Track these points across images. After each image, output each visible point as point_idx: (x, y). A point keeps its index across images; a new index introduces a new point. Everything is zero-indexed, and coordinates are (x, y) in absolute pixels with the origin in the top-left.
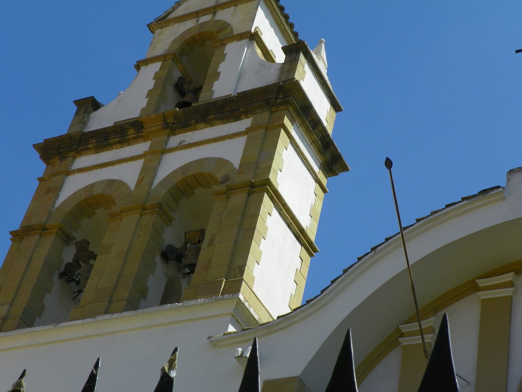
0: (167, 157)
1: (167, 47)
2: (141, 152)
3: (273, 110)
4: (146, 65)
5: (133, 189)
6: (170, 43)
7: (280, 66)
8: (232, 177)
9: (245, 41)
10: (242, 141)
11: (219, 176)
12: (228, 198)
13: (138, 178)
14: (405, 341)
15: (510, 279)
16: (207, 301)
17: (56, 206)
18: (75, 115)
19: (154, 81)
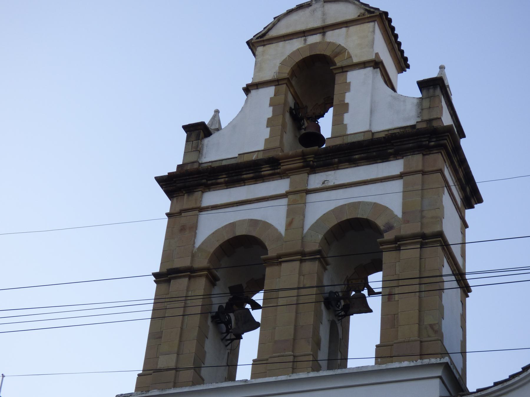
0: (311, 197)
1: (276, 69)
2: (283, 191)
3: (425, 153)
4: (257, 88)
6: (278, 65)
7: (416, 101)
8: (395, 225)
9: (369, 71)
10: (398, 185)
11: (380, 223)
13: (287, 221)
18: (187, 141)
19: (271, 108)
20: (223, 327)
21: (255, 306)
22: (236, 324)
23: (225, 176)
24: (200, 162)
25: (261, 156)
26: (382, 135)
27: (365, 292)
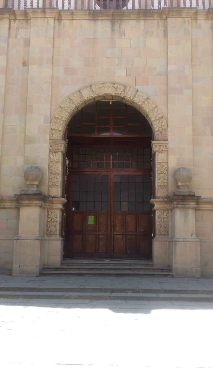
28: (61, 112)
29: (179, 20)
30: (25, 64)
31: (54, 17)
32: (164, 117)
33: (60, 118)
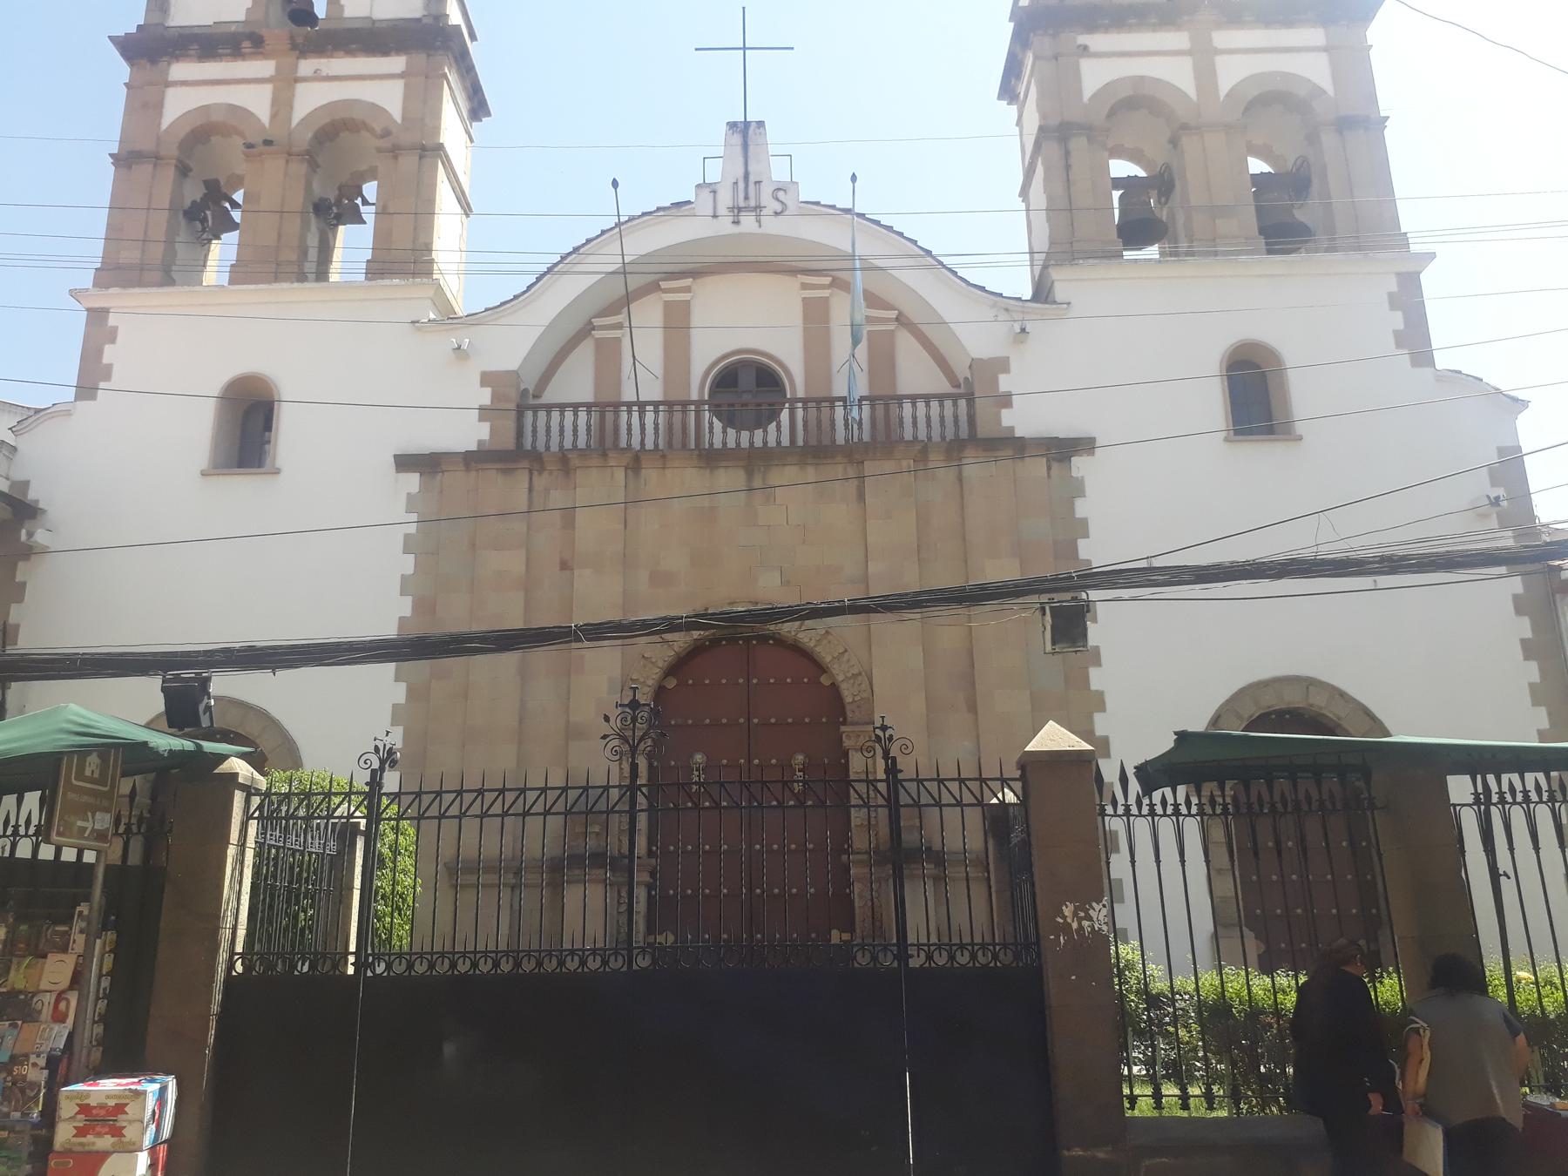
0: (300, 87)
5: (267, 125)
10: (398, 87)
11: (378, 129)
12: (396, 158)
14: (597, 334)
15: (689, 284)
16: (403, 283)
17: (165, 125)
20: (198, 225)
21: (235, 205)
22: (213, 223)
23: (196, 47)
24: (167, 25)
25: (241, 29)
26: (384, 25)
27: (359, 201)
28: (645, 666)
29: (889, 466)
30: (565, 566)
31: (624, 464)
32: (863, 673)
33: (642, 680)
